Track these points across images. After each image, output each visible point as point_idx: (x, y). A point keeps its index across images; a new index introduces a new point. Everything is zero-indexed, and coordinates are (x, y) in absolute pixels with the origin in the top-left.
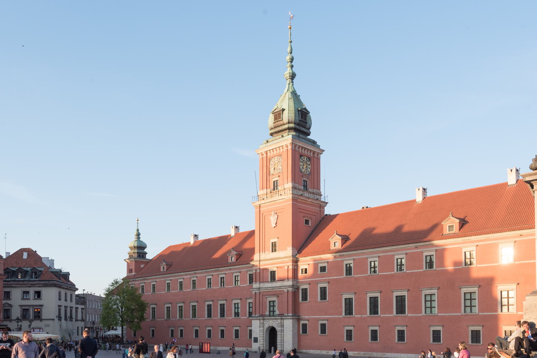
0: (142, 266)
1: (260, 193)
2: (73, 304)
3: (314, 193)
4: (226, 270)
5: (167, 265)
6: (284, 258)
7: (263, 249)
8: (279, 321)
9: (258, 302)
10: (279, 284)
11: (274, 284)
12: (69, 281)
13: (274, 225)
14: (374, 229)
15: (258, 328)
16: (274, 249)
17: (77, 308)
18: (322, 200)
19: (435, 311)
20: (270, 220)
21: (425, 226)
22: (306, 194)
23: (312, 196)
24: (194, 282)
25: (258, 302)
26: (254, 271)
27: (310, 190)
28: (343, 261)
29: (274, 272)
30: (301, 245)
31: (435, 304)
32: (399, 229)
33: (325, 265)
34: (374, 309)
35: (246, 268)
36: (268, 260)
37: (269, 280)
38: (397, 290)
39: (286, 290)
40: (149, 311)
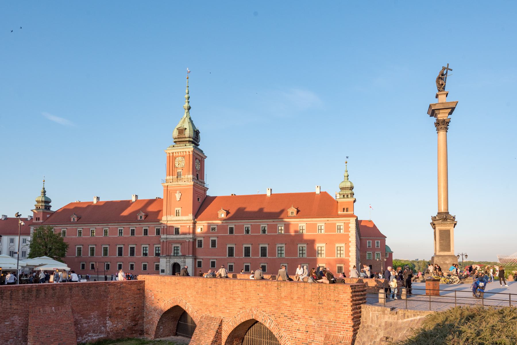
0: (48, 216)
1: (168, 178)
4: (137, 225)
5: (78, 217)
6: (187, 220)
8: (182, 259)
9: (165, 247)
10: (182, 236)
11: (178, 236)
13: (178, 199)
14: (245, 208)
19: (284, 256)
20: (175, 196)
21: (278, 210)
23: (200, 183)
24: (106, 232)
25: (165, 247)
26: (162, 227)
28: (228, 225)
29: (178, 229)
30: (197, 214)
31: (284, 252)
32: (261, 210)
33: (216, 227)
34: (247, 253)
35: (154, 224)
36: (173, 221)
38: (262, 244)
39: (187, 241)
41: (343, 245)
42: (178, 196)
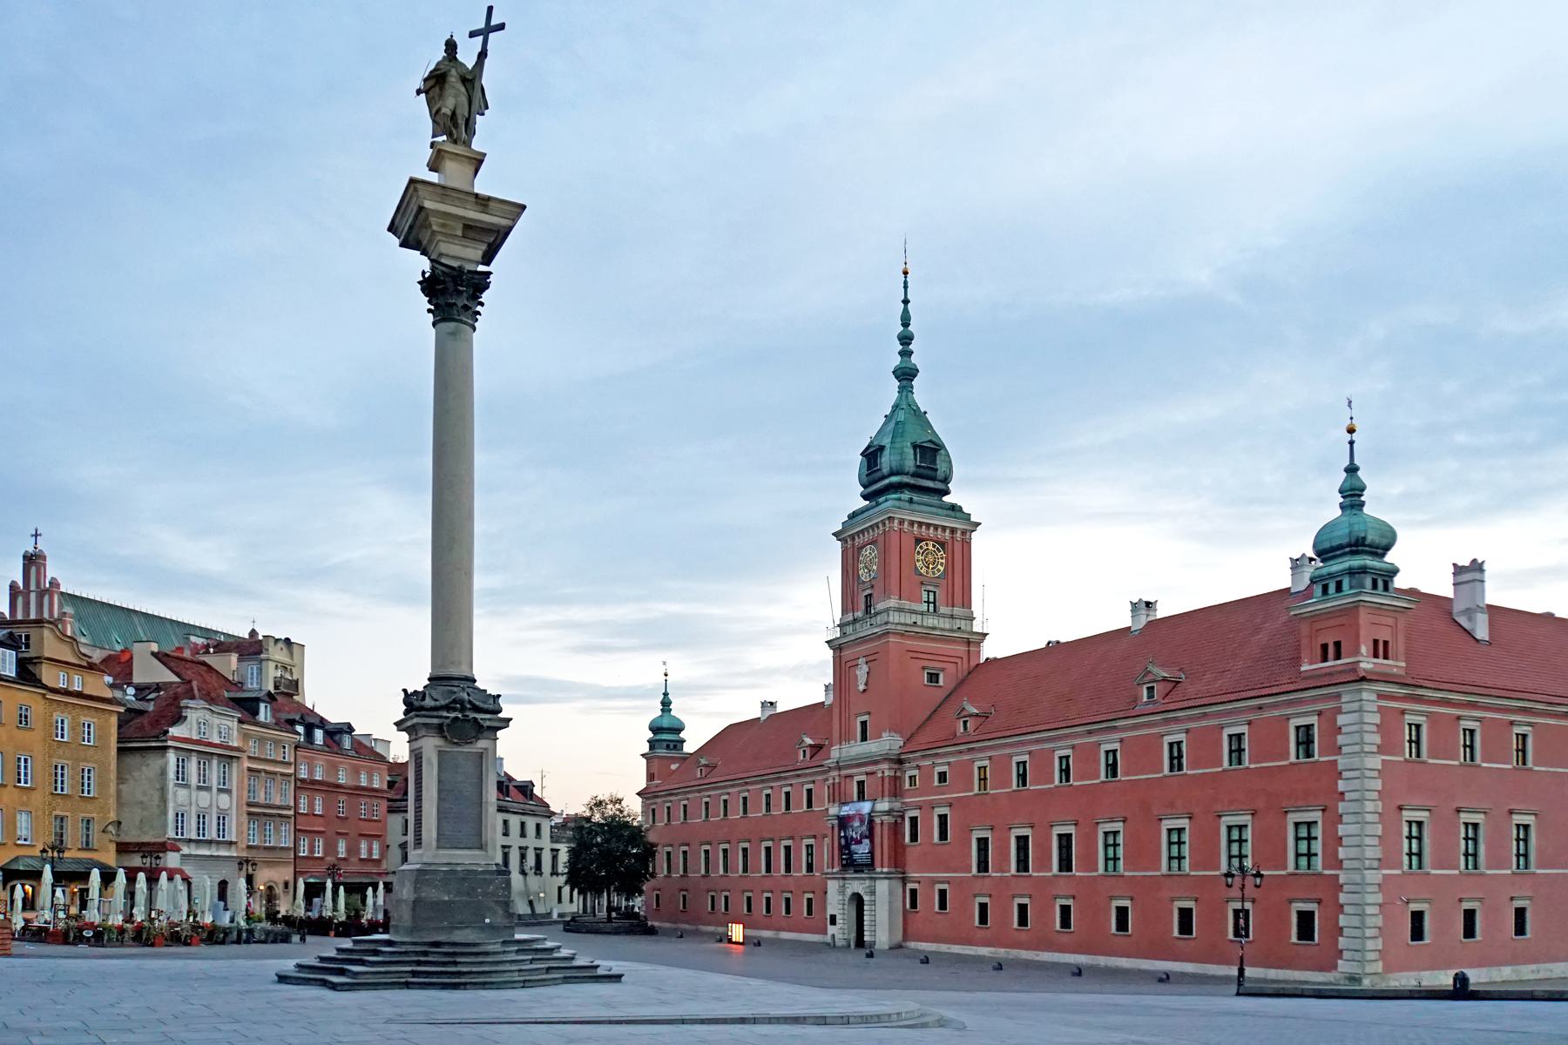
0: (674, 767)
2: (546, 843)
3: (952, 617)
7: (846, 737)
12: (532, 796)
13: (861, 687)
15: (835, 903)
16: (864, 738)
17: (555, 851)
18: (977, 628)
22: (931, 621)
23: (946, 623)
27: (943, 610)
37: (855, 797)
39: (878, 821)
40: (661, 858)
41: (1316, 816)
42: (862, 672)
